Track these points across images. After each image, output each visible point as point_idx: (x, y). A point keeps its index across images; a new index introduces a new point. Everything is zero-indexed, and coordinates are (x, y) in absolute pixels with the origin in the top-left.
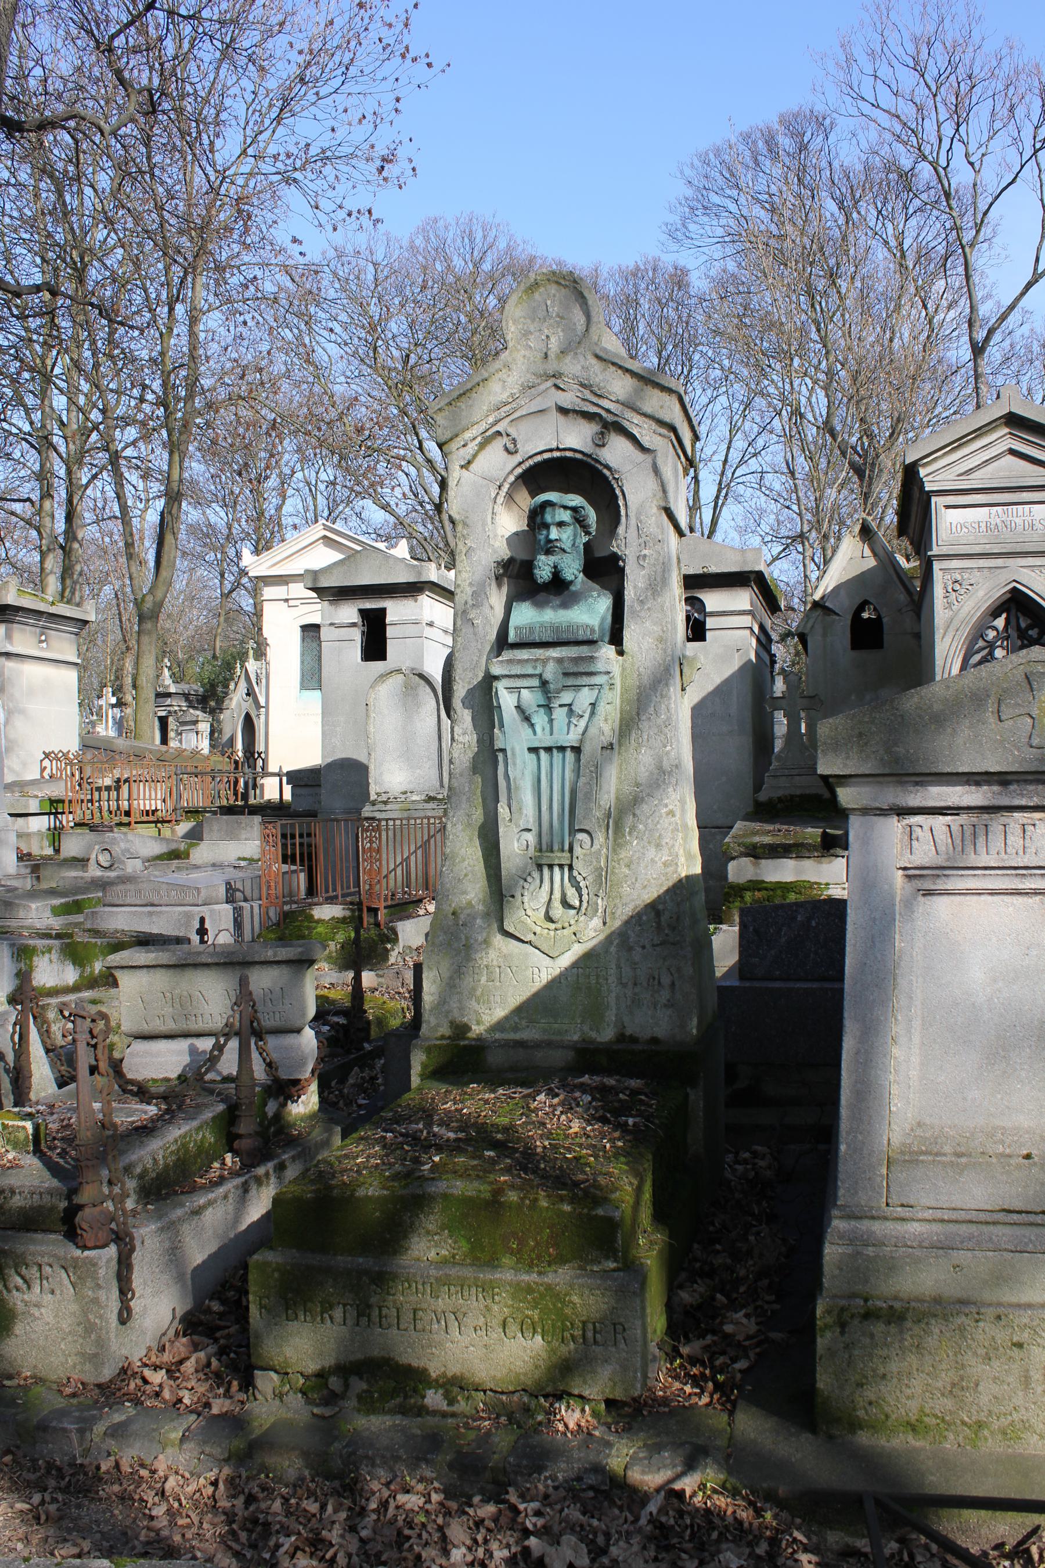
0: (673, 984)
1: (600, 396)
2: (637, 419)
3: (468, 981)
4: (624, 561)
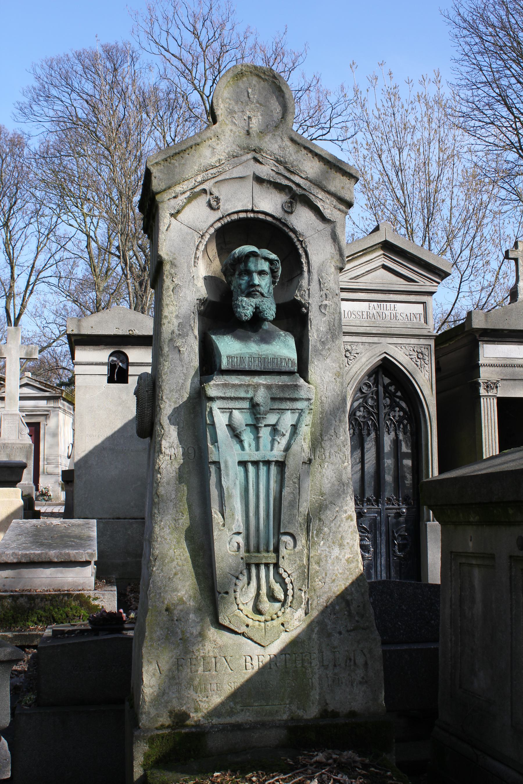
0: (366, 664)
1: (292, 172)
2: (321, 195)
3: (186, 671)
4: (307, 309)
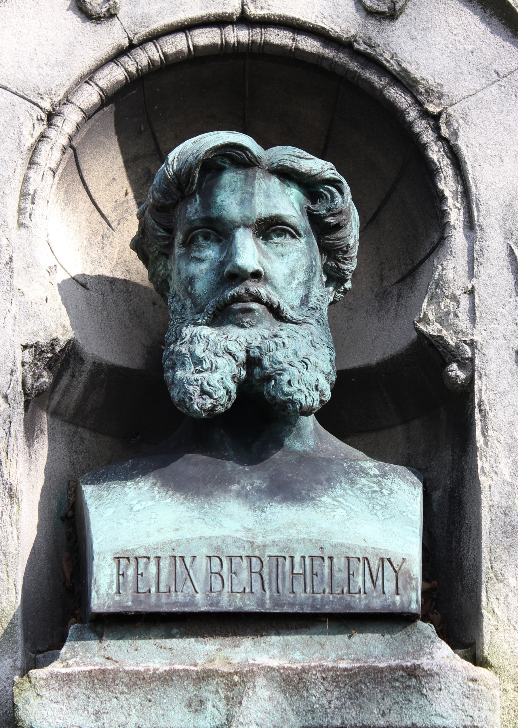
4: (468, 364)
